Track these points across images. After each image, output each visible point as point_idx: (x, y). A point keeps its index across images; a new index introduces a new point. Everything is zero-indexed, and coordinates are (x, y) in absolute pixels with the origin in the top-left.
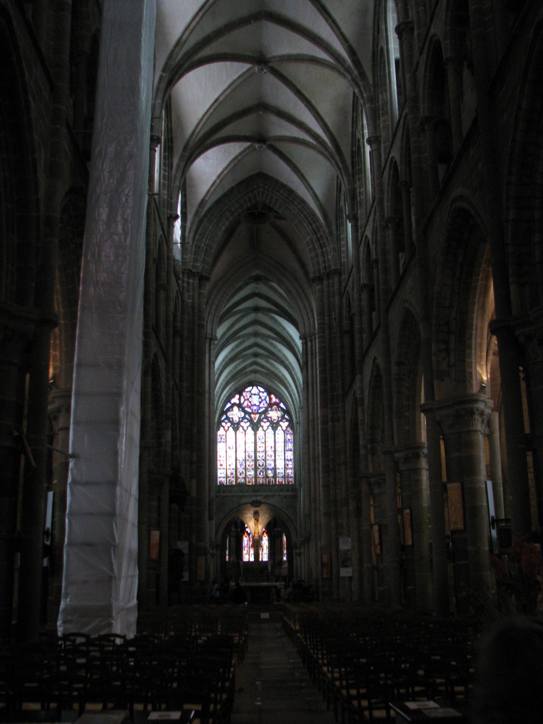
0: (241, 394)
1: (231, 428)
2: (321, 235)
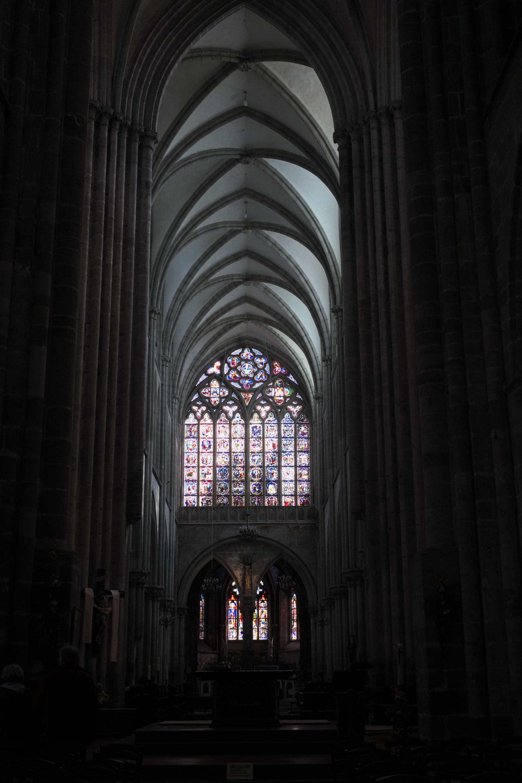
1: (206, 416)
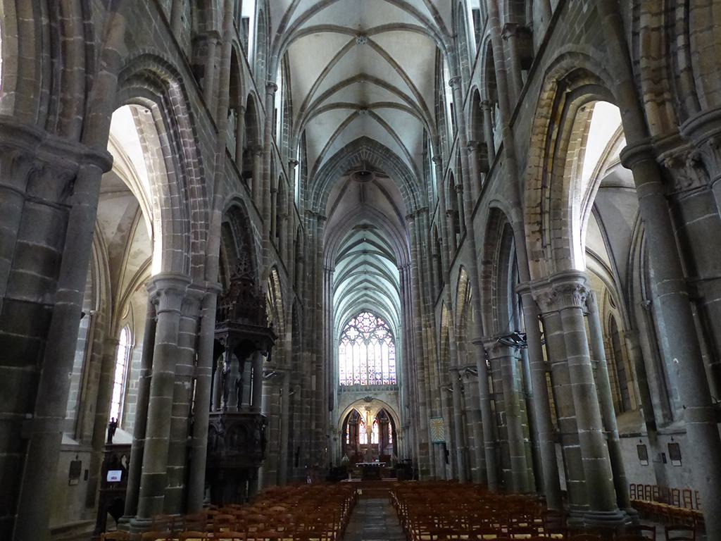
0: (355, 318)
2: (412, 183)
